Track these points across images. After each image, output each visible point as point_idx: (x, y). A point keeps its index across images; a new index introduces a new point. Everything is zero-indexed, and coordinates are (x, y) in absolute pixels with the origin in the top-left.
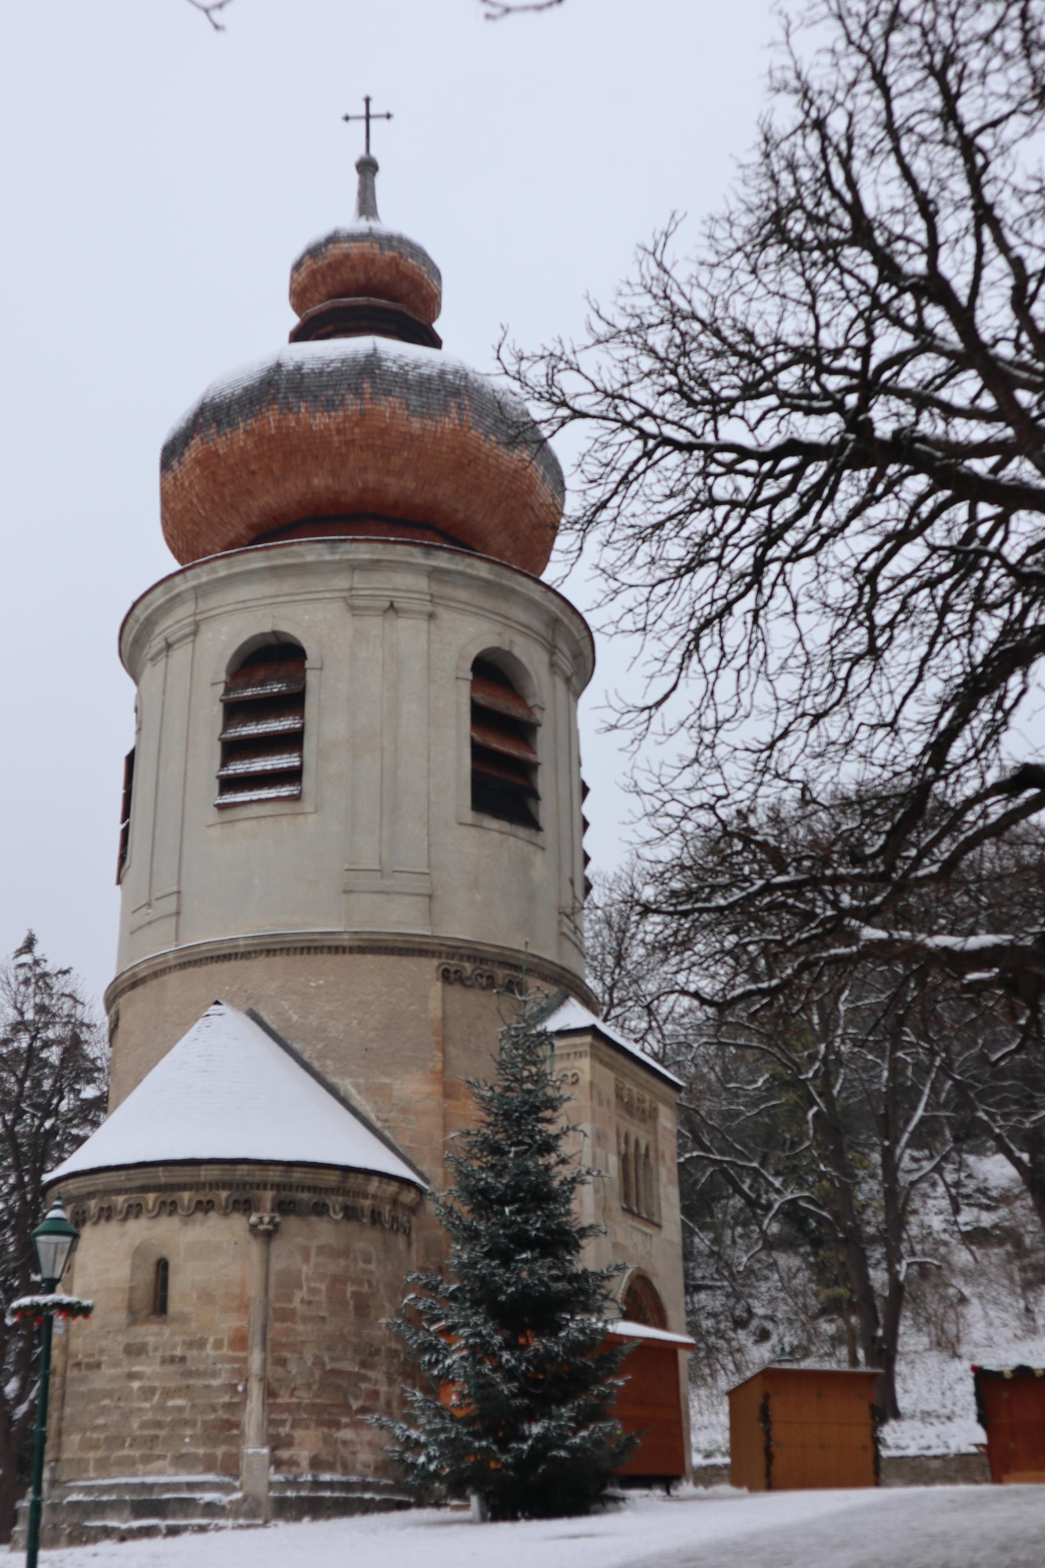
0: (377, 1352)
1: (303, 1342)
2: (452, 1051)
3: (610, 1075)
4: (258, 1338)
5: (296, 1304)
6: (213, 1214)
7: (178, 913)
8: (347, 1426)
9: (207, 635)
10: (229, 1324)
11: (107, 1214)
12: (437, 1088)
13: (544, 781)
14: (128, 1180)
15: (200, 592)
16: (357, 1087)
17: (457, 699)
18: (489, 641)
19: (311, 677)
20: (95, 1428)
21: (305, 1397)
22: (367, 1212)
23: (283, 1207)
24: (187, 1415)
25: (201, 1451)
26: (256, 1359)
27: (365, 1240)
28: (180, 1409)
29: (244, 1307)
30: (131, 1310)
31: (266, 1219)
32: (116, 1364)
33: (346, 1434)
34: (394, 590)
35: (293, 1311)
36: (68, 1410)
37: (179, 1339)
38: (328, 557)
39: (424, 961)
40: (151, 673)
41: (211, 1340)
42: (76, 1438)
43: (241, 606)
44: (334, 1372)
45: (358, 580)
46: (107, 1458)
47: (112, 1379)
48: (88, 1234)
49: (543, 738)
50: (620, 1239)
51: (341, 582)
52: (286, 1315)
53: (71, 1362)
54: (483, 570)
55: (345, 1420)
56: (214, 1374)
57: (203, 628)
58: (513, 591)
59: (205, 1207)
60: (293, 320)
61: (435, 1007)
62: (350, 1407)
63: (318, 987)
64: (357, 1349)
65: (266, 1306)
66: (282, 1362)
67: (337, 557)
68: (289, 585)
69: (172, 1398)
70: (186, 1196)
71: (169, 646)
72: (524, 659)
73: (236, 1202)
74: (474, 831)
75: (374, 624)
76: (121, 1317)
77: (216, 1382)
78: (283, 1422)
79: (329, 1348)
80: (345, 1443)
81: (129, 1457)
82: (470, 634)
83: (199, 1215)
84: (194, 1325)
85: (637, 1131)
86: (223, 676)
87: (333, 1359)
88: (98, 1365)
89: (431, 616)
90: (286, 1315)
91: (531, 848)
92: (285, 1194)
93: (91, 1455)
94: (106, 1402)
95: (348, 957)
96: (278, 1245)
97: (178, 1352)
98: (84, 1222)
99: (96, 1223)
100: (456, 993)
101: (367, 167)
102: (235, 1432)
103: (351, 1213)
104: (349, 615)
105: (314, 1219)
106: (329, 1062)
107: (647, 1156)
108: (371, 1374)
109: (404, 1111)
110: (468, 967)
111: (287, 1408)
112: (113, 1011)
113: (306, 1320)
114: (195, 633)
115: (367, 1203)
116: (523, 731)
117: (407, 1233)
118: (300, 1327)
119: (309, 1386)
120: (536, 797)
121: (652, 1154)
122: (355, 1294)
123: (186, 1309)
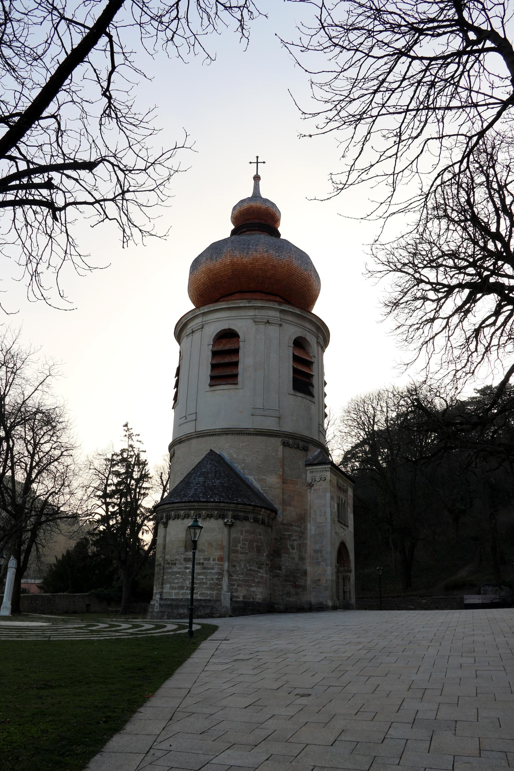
0: (263, 564)
1: (241, 560)
2: (286, 468)
3: (336, 478)
4: (227, 558)
5: (239, 548)
6: (212, 519)
7: (196, 420)
8: (254, 586)
9: (206, 329)
10: (218, 553)
11: (177, 517)
12: (281, 480)
13: (315, 381)
14: (185, 506)
15: (204, 314)
16: (255, 479)
17: (288, 352)
18: (299, 334)
19: (241, 344)
20: (174, 583)
21: (241, 577)
22: (261, 520)
23: (235, 517)
24: (204, 581)
25: (209, 592)
26: (226, 565)
27: (260, 529)
28: (202, 579)
29: (222, 548)
30: (185, 547)
31: (230, 521)
32: (181, 564)
33: (254, 589)
34: (269, 316)
35: (238, 550)
36: (165, 577)
37: (201, 557)
38: (247, 305)
39: (277, 439)
40: (185, 340)
41: (212, 558)
42: (168, 586)
43: (218, 320)
44: (250, 569)
45: (257, 312)
46: (178, 593)
47: (180, 568)
48: (171, 522)
49: (315, 366)
50: (337, 531)
51: (251, 313)
52: (236, 552)
53: (166, 562)
54: (297, 311)
55: (253, 585)
56: (213, 569)
57: (205, 326)
58: (306, 318)
59: (210, 516)
60: (233, 227)
61: (280, 454)
62: (255, 581)
63: (243, 446)
64: (257, 563)
65: (229, 548)
66: (234, 566)
67: (250, 305)
68: (234, 313)
69: (199, 575)
70: (204, 512)
71: (193, 332)
72: (309, 340)
73: (220, 515)
74: (294, 397)
75: (262, 327)
76: (182, 549)
77: (213, 571)
78: (234, 585)
79: (249, 562)
80: (253, 592)
81: (186, 593)
82: (293, 331)
83: (208, 519)
84: (206, 553)
85: (342, 496)
86: (212, 343)
87: (250, 566)
88: (175, 564)
89: (281, 325)
90: (236, 552)
91: (311, 402)
93: (174, 591)
94: (178, 575)
95: (252, 437)
96: (233, 530)
97: (201, 561)
98: (170, 519)
99: (174, 519)
100: (287, 449)
101: (257, 178)
102: (219, 587)
103: (256, 520)
104: (254, 324)
105: (244, 521)
106: (246, 471)
107: (344, 504)
108: (261, 571)
109: (270, 487)
110: (291, 441)
111: (236, 580)
112: (172, 450)
113: (241, 553)
114: (202, 328)
115: (261, 517)
116: (309, 364)
117: (271, 527)
118: (240, 556)
119: (242, 574)
120: (313, 386)
121: (346, 504)
122: (257, 546)
123: (204, 548)
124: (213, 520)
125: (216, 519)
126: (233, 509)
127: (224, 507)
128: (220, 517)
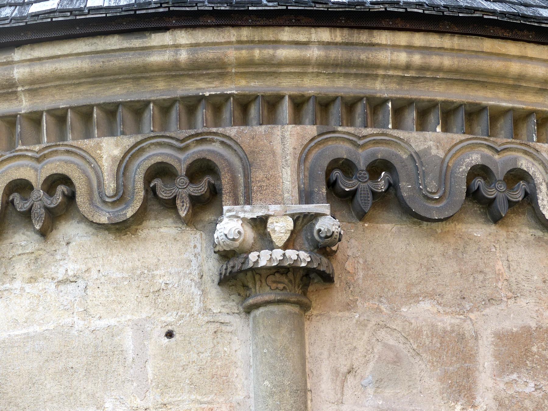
6: (72, 233)
31: (281, 228)
73: (161, 171)
92: (358, 140)
105: (479, 231)
124: (76, 247)
125: (122, 228)
126: (313, 85)
127: (197, 69)
128: (158, 204)
